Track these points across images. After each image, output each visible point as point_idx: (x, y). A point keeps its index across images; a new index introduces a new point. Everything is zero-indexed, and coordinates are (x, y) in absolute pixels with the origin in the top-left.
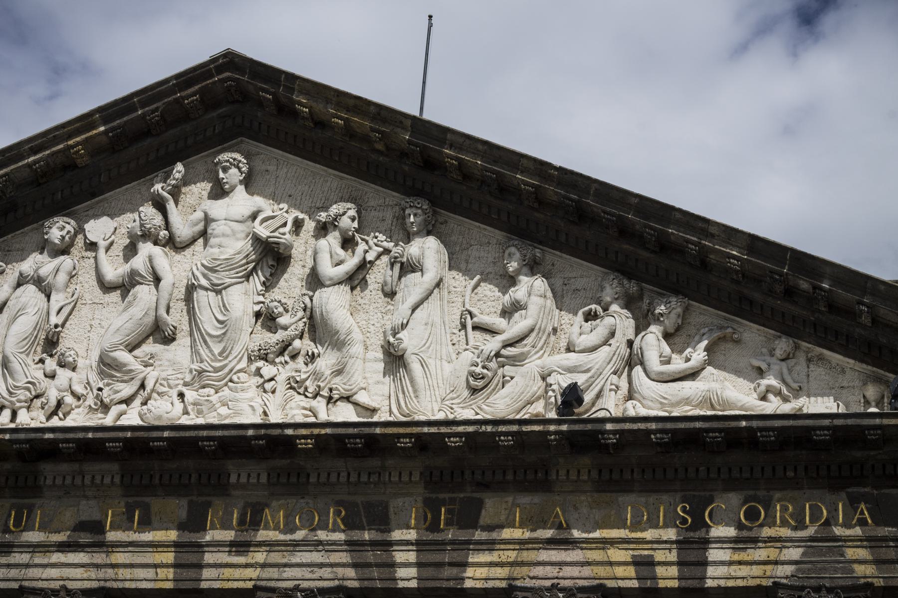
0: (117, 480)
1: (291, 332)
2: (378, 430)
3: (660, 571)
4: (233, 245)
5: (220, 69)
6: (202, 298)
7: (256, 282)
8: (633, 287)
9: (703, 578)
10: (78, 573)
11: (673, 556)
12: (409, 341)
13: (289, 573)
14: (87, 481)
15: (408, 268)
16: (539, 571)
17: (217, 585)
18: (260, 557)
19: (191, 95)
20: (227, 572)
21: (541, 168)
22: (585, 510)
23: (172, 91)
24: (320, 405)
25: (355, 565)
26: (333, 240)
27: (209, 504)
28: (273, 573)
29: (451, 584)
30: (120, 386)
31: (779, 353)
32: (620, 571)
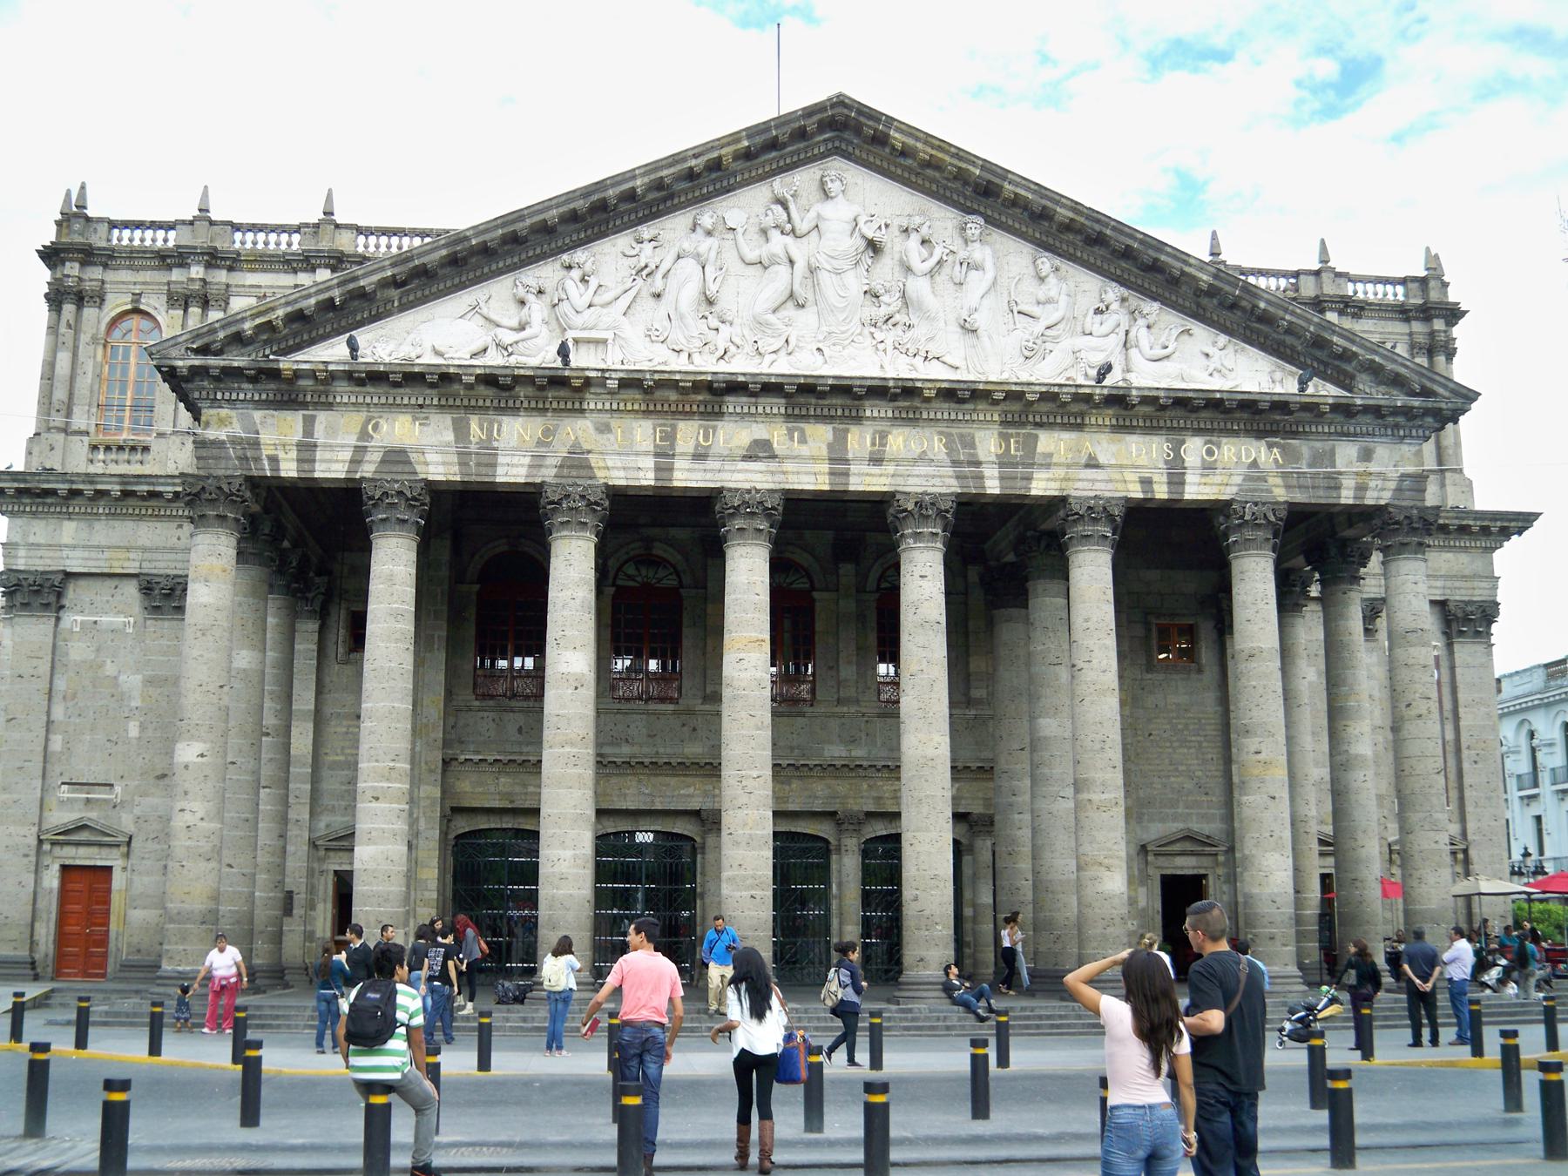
0: (783, 411)
1: (891, 310)
2: (981, 387)
3: (1156, 487)
4: (840, 242)
5: (833, 106)
6: (823, 276)
7: (862, 269)
8: (1125, 292)
9: (1183, 493)
10: (758, 477)
11: (1165, 479)
12: (980, 320)
13: (911, 481)
14: (760, 410)
15: (971, 266)
16: (1079, 485)
17: (861, 488)
18: (891, 469)
19: (811, 124)
20: (868, 480)
21: (1076, 207)
22: (1105, 445)
23: (798, 119)
24: (919, 360)
25: (957, 477)
26: (914, 240)
27: (847, 431)
28: (900, 481)
29: (1022, 492)
30: (772, 340)
31: (1220, 344)
32: (1131, 487)
